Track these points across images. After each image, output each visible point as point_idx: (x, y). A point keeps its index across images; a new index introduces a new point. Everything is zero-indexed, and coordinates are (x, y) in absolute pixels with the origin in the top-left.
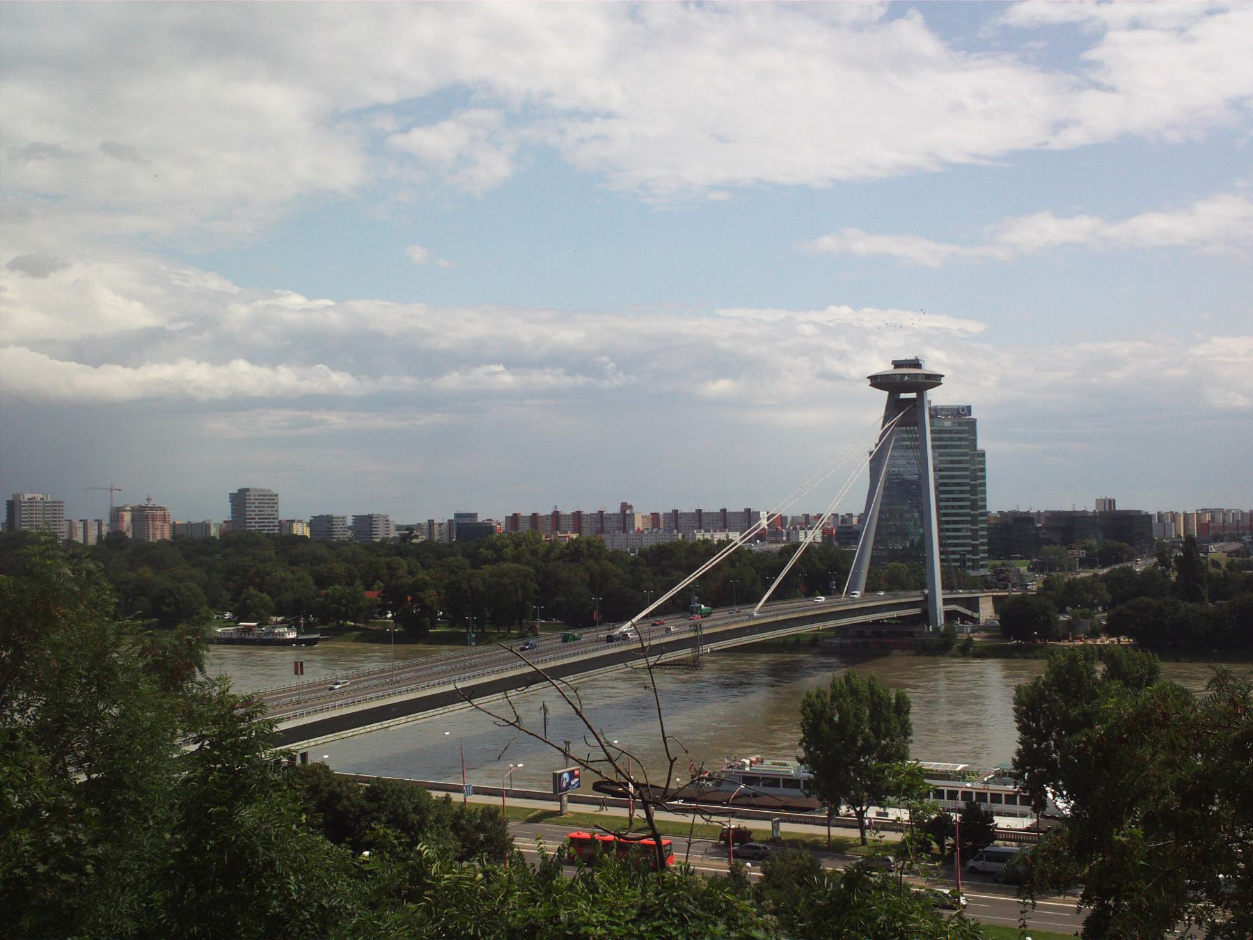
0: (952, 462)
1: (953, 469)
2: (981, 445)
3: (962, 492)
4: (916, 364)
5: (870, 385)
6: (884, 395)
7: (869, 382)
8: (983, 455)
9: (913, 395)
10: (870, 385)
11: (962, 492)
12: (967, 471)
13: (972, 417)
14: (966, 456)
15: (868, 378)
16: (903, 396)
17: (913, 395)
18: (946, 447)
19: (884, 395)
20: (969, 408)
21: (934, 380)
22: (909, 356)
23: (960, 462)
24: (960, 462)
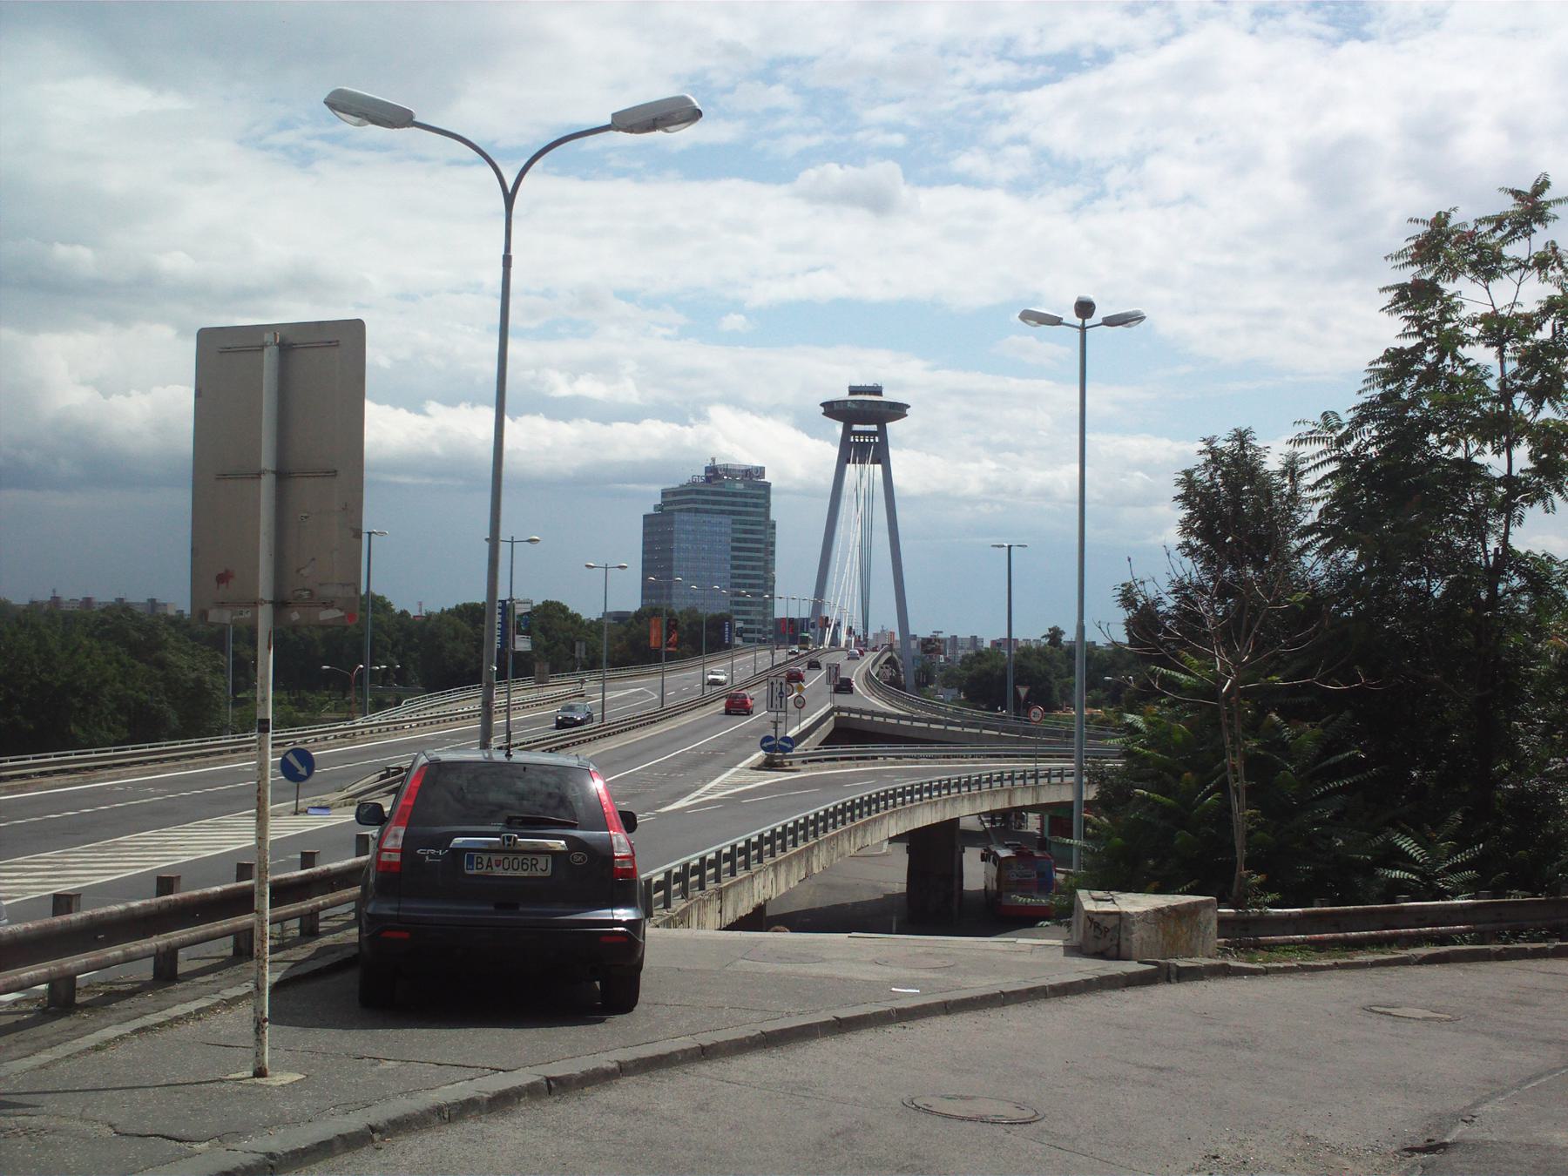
0: (746, 532)
1: (745, 540)
2: (774, 515)
3: (753, 568)
4: (877, 391)
5: (823, 414)
6: (838, 427)
7: (822, 409)
8: (774, 527)
9: (874, 428)
10: (823, 414)
11: (753, 568)
12: (760, 543)
13: (765, 480)
14: (760, 525)
15: (822, 405)
16: (856, 427)
17: (874, 428)
18: (740, 513)
19: (838, 427)
20: (761, 471)
21: (898, 411)
22: (868, 382)
23: (752, 532)
24: (752, 532)
